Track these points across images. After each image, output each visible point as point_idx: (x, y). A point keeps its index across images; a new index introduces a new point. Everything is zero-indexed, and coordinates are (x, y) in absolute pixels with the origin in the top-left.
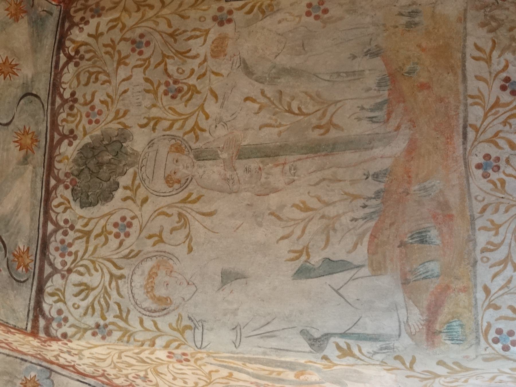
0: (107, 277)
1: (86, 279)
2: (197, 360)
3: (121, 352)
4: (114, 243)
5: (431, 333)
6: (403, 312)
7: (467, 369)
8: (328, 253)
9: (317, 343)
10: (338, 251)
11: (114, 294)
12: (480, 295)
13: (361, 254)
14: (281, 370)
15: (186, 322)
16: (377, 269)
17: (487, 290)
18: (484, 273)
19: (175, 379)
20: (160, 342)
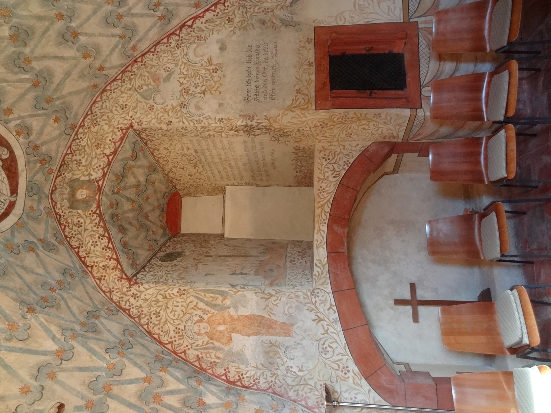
0: (164, 273)
1: (156, 273)
2: (188, 293)
3: (160, 290)
4: (169, 268)
5: (271, 284)
6: (263, 282)
7: (282, 291)
8: (242, 271)
9: (233, 286)
10: (245, 271)
11: (165, 276)
12: (287, 279)
13: (253, 272)
14: (218, 296)
15: (189, 281)
16: (257, 273)
17: (289, 279)
18: (288, 276)
19: (171, 312)
20: (177, 285)
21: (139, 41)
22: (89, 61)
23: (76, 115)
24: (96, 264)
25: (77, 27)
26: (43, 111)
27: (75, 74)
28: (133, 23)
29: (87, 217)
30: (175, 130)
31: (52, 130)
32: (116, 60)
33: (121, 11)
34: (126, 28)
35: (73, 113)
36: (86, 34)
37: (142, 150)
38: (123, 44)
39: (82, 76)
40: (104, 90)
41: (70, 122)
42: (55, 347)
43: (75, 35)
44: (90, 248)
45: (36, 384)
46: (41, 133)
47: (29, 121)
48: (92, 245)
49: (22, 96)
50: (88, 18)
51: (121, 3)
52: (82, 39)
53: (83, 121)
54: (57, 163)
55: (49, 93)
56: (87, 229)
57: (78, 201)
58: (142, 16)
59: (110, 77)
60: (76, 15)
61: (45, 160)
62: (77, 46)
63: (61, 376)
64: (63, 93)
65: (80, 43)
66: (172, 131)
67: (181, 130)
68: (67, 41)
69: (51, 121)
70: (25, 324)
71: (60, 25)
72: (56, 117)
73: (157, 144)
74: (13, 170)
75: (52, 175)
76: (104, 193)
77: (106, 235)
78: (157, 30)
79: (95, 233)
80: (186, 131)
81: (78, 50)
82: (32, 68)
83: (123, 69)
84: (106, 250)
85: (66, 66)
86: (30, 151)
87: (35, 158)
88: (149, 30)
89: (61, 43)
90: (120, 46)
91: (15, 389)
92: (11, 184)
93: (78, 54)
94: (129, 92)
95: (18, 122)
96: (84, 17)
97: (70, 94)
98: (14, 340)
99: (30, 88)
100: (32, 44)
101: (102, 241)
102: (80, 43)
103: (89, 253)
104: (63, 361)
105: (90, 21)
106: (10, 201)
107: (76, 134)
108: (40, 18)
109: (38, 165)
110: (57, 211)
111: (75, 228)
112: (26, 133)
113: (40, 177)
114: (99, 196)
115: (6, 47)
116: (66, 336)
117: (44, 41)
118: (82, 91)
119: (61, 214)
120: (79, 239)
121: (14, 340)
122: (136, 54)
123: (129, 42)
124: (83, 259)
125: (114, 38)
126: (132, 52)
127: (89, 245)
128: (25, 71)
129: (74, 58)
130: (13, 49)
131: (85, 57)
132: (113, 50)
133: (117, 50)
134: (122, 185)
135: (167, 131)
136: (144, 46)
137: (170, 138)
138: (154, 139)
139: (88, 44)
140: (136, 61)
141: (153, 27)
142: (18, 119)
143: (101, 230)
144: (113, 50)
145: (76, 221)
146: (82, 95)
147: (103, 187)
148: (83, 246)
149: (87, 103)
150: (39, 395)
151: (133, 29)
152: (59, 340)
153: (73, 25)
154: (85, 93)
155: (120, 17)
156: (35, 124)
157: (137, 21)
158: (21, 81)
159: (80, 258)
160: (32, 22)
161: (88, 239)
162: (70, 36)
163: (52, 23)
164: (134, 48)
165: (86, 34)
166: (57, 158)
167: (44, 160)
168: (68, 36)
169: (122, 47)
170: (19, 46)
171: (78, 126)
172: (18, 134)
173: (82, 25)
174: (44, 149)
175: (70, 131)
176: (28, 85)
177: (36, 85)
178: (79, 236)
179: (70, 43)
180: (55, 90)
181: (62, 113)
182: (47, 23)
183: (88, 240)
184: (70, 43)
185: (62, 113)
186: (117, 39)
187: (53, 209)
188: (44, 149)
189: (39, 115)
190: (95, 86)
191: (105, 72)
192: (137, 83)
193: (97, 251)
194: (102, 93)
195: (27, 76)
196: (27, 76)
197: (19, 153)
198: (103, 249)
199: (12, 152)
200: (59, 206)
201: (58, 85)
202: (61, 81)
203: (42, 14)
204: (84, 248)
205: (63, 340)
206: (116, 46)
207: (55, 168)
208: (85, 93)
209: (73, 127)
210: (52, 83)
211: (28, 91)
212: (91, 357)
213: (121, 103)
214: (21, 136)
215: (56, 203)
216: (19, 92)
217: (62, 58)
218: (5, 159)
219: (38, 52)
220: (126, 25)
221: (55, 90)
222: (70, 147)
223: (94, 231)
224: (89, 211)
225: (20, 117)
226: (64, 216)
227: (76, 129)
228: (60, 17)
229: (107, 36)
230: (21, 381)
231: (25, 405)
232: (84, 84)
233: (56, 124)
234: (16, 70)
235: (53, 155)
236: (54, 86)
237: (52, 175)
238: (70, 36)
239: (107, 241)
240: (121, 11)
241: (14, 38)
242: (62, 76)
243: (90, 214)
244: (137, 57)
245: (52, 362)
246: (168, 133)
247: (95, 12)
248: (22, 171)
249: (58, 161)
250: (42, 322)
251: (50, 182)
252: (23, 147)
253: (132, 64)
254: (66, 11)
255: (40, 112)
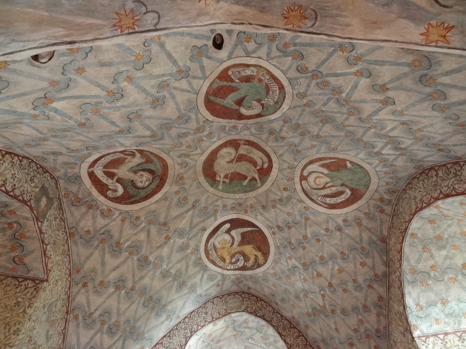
21: (78, 325)
22: (97, 282)
23: (76, 243)
24: (2, 162)
25: (120, 293)
26: (102, 232)
27: (99, 267)
28: (92, 329)
29: (32, 191)
30: (20, 320)
31: (87, 224)
32: (81, 299)
33: (106, 326)
34: (94, 321)
35: (79, 244)
36: (113, 294)
37: (13, 269)
38: (86, 312)
39: (94, 270)
40: (70, 275)
41: (77, 237)
42: (55, 105)
43: (117, 288)
44: (14, 170)
45: (69, 76)
46: (94, 218)
47: (107, 221)
48: (15, 174)
49: (121, 232)
50: (119, 302)
51: (110, 330)
52: (112, 290)
53: (68, 244)
54: (65, 204)
55: (106, 245)
56: (26, 182)
57: (42, 196)
58: (92, 339)
59: (74, 285)
60: (126, 298)
61: (77, 202)
62: (112, 284)
63: (44, 84)
64: (97, 251)
65: (111, 286)
66: (21, 315)
67: (17, 326)
68: (119, 281)
69: (91, 229)
70: (85, 114)
71: (129, 284)
72: (90, 234)
73: (8, 288)
74: (98, 186)
75: (63, 193)
76: (31, 219)
77: (11, 193)
78: (73, 343)
79: (19, 185)
80: (12, 331)
81: (109, 282)
82: (126, 251)
83: (70, 299)
84: (4, 181)
85: (108, 268)
86: (93, 203)
87: (87, 200)
88: (78, 338)
89: (121, 276)
90: (87, 309)
91: (91, 72)
92: (96, 177)
93: (107, 280)
94: (59, 293)
95: (114, 217)
96: (122, 300)
97: (92, 254)
98: (93, 103)
99: (120, 240)
100: (136, 263)
101: (11, 185)
102: (111, 286)
103: (12, 165)
104: (44, 96)
105: (116, 303)
106: (93, 168)
107: (66, 233)
108: (142, 278)
109: (80, 196)
110: (48, 174)
111: (32, 174)
112: (105, 214)
113: (74, 188)
114: (35, 215)
115: (146, 251)
116: (44, 115)
117: (131, 270)
118: (85, 262)
119: (45, 175)
120: (25, 169)
121: (93, 103)
122: (72, 316)
123: (84, 317)
124: (13, 155)
125: (95, 308)
126: (75, 314)
127: (16, 172)
128: (129, 247)
129: (107, 276)
130: (142, 253)
131: (102, 282)
132: (88, 302)
133: (86, 305)
134: (9, 232)
135: (24, 311)
136: (71, 327)
137: (9, 307)
138: (18, 290)
139: (107, 290)
140: (67, 312)
141: (78, 341)
142: (115, 218)
143: (17, 192)
144: (88, 302)
145: (36, 180)
146: (82, 259)
147: (36, 223)
148: (19, 167)
149: (75, 257)
150: (65, 68)
151: (88, 326)
152: (50, 111)
153: (123, 292)
154: (82, 262)
155: (103, 323)
156: (101, 222)
157: (92, 332)
158: (128, 240)
159: (15, 155)
160: (143, 273)
161: (20, 176)
162: (119, 285)
163: (134, 282)
164: (76, 317)
165: (113, 294)
166: (68, 207)
167: (79, 202)
168: (121, 284)
169: (85, 310)
170: (141, 257)
171: (69, 238)
172: (110, 210)
173: (119, 296)
174: (84, 209)
175: (73, 230)
176: (122, 241)
177: (118, 243)
178: (26, 171)
179: (116, 281)
180: (104, 249)
181: (88, 238)
182: (136, 279)
183: (20, 175)
184: (116, 281)
185: (88, 238)
186: (92, 311)
187: (51, 172)
188: (84, 209)
189: (103, 227)
190: (78, 271)
191: (80, 285)
192: (59, 304)
193: (9, 173)
194: (70, 273)
195: (126, 245)
196: (126, 245)
197: (101, 199)
198: (6, 179)
199: (106, 196)
200: (49, 178)
201: (104, 254)
202: (104, 257)
203: (142, 281)
204: (18, 165)
205: (47, 112)
206: (89, 307)
207: (64, 200)
208: (82, 262)
209: (71, 235)
210: (109, 252)
211: (120, 238)
212: (11, 107)
213: (59, 281)
214: (106, 209)
215: (51, 178)
216: (124, 234)
217: (115, 269)
218: (108, 190)
219: (129, 262)
220: (95, 323)
221: (104, 249)
222: (64, 221)
223: (21, 186)
224: (34, 197)
225: (114, 220)
226: (43, 175)
227: (68, 235)
228: (133, 289)
229: (99, 306)
230: (85, 77)
231: (80, 60)
232: (87, 266)
233: (86, 229)
234: (134, 244)
235: (73, 208)
236: (107, 250)
237: (63, 193)
238: (119, 285)
239: (8, 189)
240: (106, 326)
241: (146, 259)
242: (106, 260)
243: (32, 196)
244: (69, 315)
245: (54, 93)
246: (21, 311)
247: (118, 309)
248: (91, 188)
249: (65, 206)
250: (70, 119)
251: (62, 189)
252: (100, 203)
253: (67, 308)
254: (133, 294)
255: (103, 230)
